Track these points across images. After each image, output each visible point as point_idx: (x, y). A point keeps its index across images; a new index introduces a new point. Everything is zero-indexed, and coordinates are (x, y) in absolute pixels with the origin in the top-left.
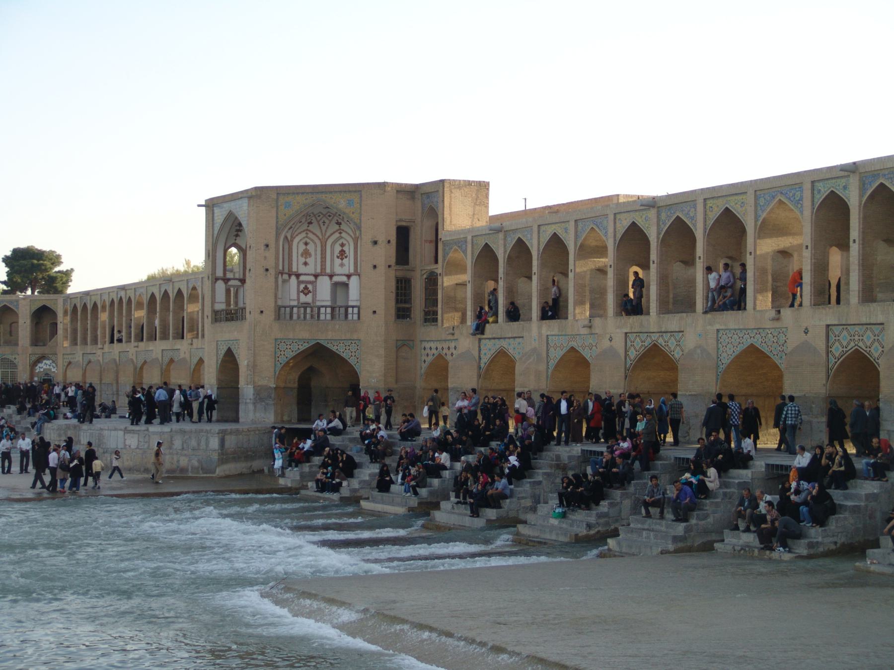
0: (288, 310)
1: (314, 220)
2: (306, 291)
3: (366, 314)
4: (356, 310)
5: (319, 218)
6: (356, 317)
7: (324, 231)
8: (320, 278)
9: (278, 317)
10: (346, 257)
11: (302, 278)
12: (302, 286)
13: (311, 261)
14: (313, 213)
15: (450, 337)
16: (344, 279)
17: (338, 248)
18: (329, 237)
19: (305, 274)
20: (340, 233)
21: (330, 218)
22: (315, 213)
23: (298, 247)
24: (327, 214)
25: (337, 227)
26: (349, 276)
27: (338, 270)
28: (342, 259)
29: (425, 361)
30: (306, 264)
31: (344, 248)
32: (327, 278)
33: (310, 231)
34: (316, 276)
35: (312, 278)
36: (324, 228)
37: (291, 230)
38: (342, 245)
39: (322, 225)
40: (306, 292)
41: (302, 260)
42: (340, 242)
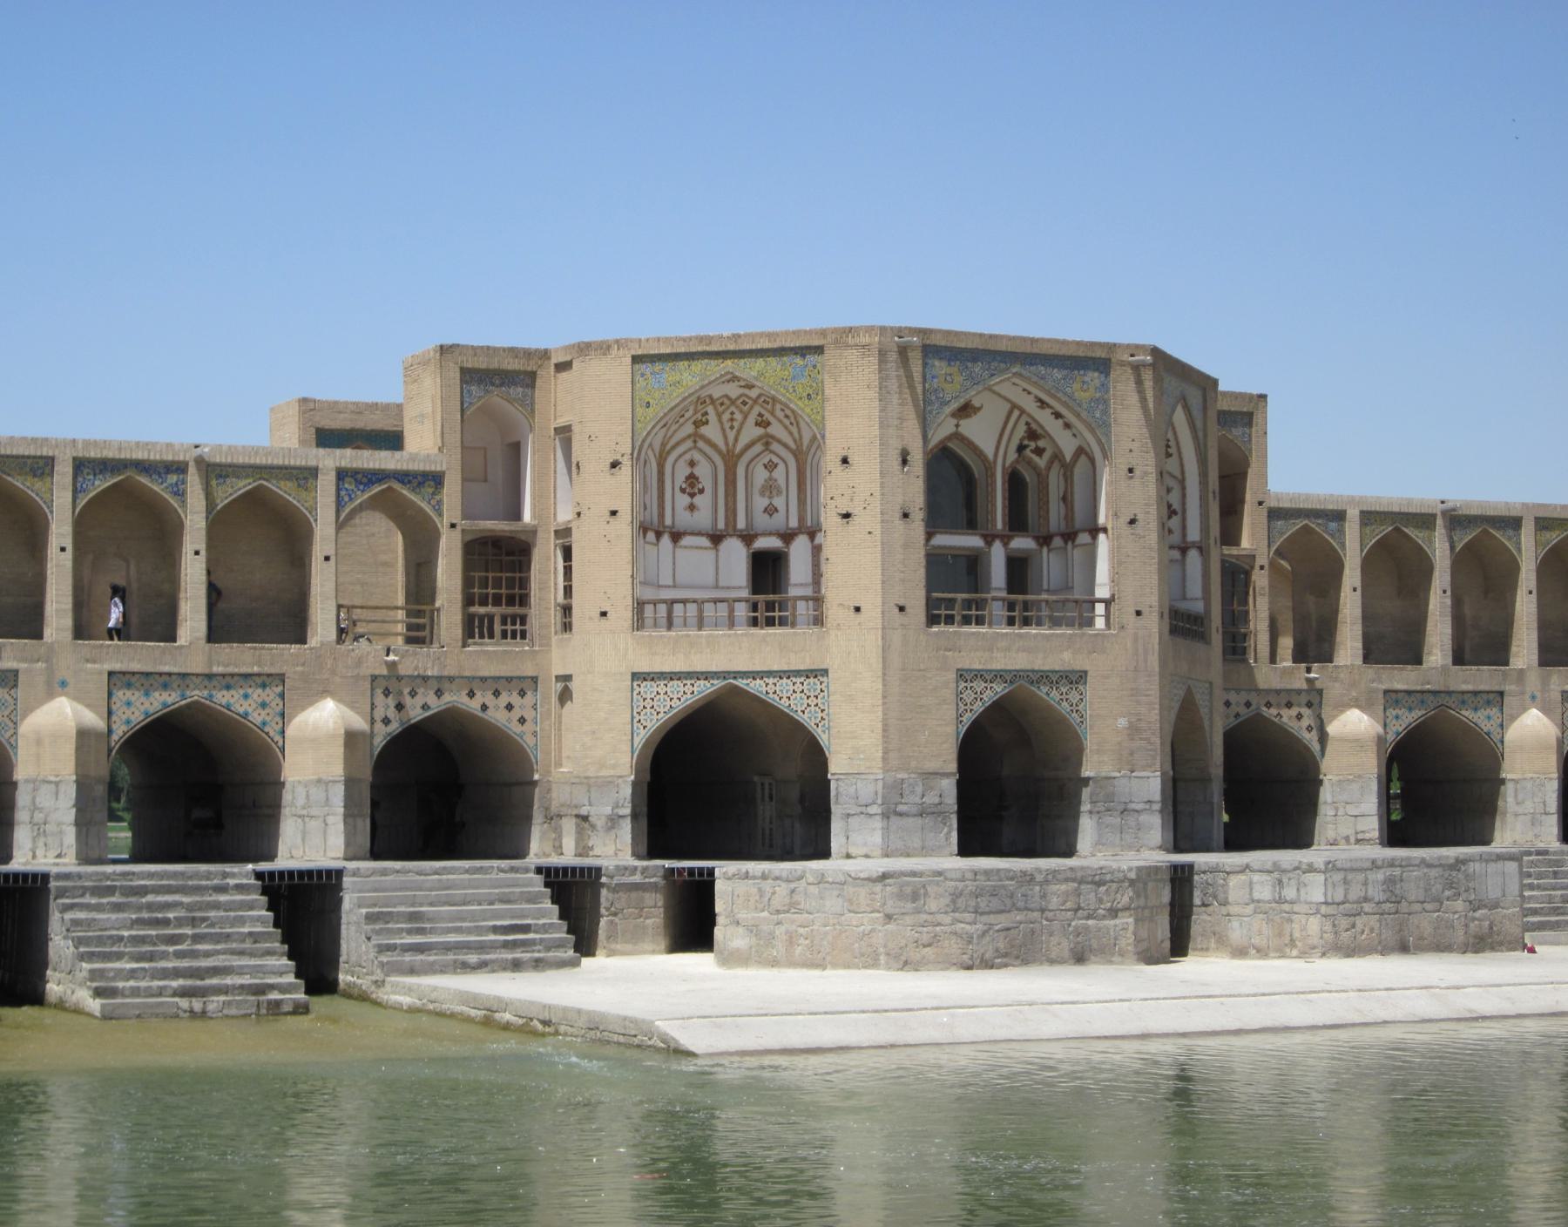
0: (662, 608)
1: (712, 417)
5: (721, 409)
10: (779, 493)
11: (687, 541)
13: (702, 501)
14: (710, 397)
19: (692, 534)
20: (767, 444)
21: (746, 408)
22: (716, 396)
24: (738, 398)
25: (760, 431)
26: (788, 537)
27: (762, 521)
30: (692, 507)
33: (703, 437)
35: (705, 542)
37: (665, 429)
38: (770, 467)
39: (727, 426)
41: (683, 500)
42: (766, 458)
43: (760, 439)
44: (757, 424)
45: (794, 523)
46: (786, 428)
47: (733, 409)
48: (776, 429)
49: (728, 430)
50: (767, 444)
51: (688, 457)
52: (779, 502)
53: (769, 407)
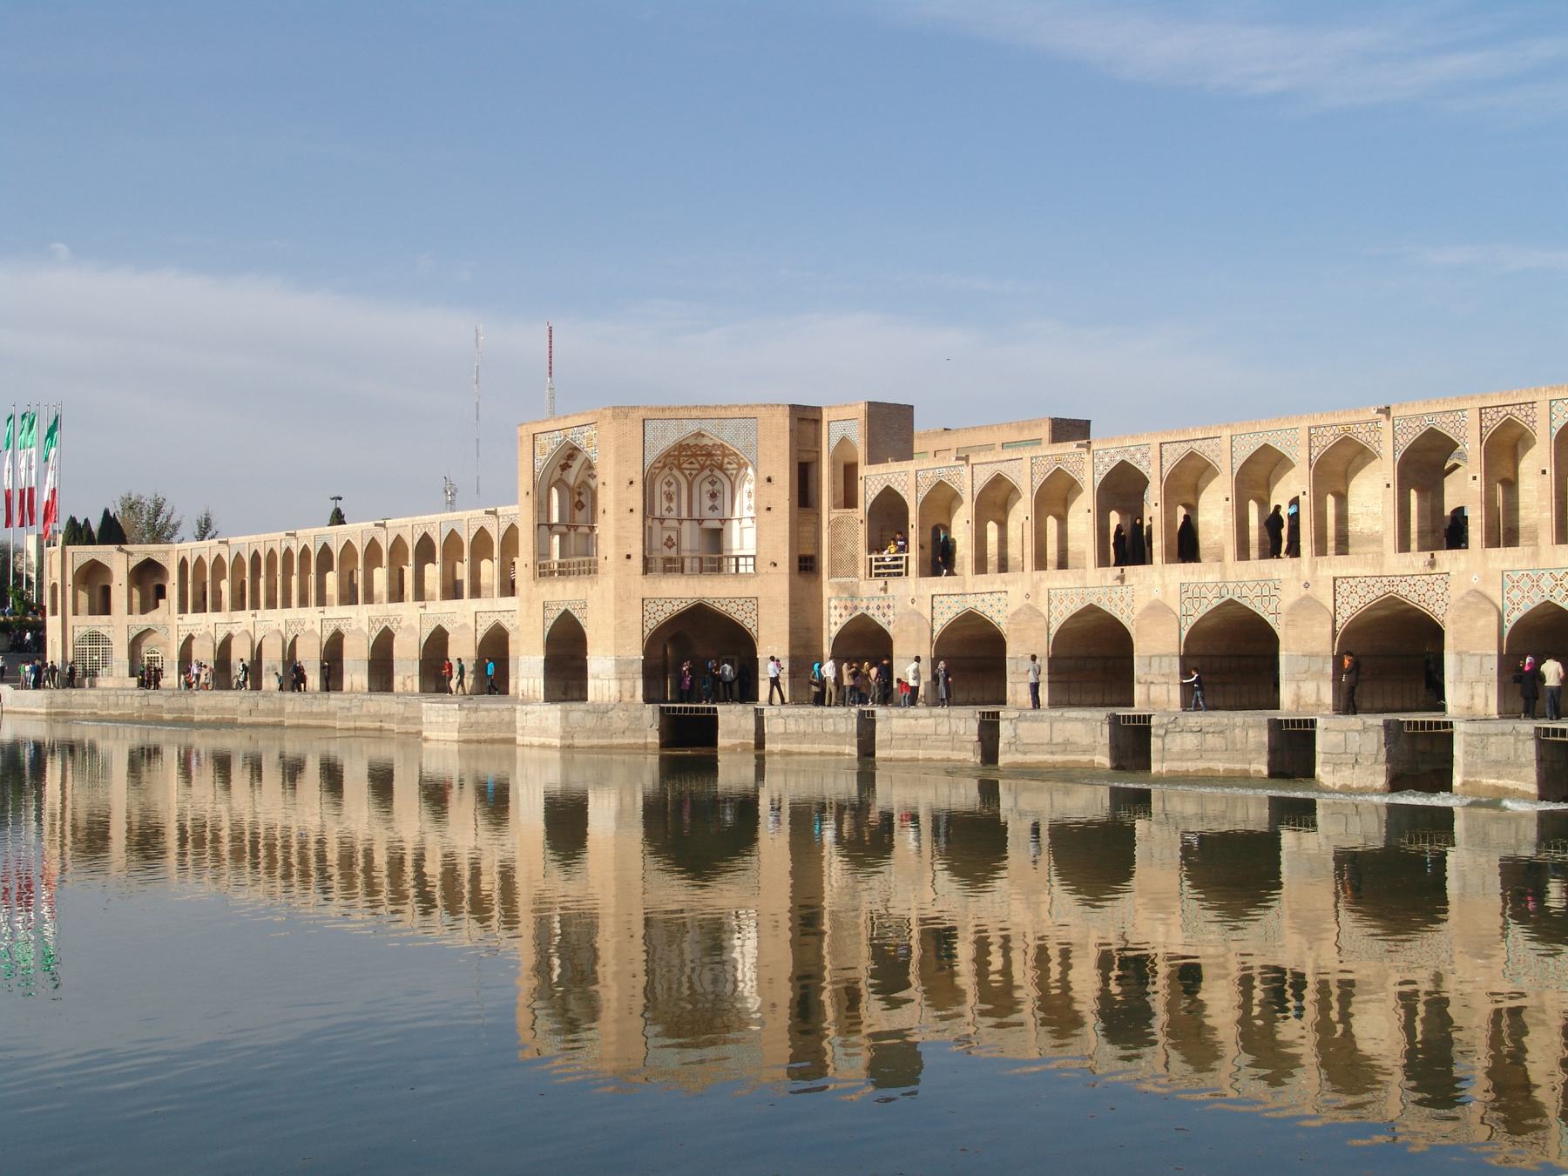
2: (670, 543)
3: (765, 567)
4: (750, 561)
6: (750, 569)
8: (684, 522)
9: (647, 568)
11: (666, 523)
12: (666, 536)
13: (674, 505)
15: (882, 594)
16: (717, 525)
23: (660, 489)
26: (723, 521)
27: (707, 513)
29: (836, 624)
32: (695, 523)
34: (680, 521)
35: (676, 524)
38: (713, 483)
40: (669, 543)
45: (727, 515)
52: (716, 503)
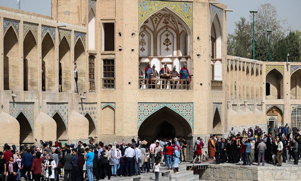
7: (155, 26)
10: (170, 44)
17: (164, 38)
18: (159, 31)
20: (167, 28)
24: (158, 14)
25: (164, 25)
28: (167, 45)
31: (169, 38)
33: (146, 26)
36: (155, 25)
38: (167, 35)
39: (155, 22)
42: (166, 33)
43: (165, 27)
44: (163, 22)
46: (172, 24)
47: (156, 17)
48: (170, 24)
49: (155, 24)
50: (167, 28)
51: (141, 34)
53: (168, 18)
